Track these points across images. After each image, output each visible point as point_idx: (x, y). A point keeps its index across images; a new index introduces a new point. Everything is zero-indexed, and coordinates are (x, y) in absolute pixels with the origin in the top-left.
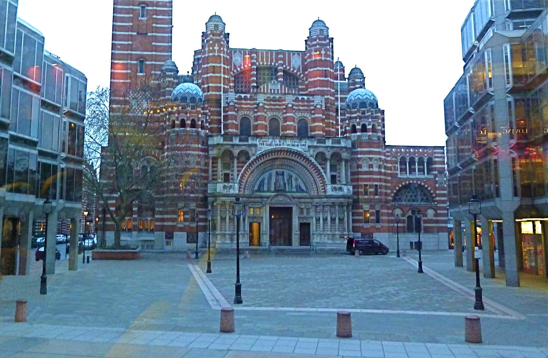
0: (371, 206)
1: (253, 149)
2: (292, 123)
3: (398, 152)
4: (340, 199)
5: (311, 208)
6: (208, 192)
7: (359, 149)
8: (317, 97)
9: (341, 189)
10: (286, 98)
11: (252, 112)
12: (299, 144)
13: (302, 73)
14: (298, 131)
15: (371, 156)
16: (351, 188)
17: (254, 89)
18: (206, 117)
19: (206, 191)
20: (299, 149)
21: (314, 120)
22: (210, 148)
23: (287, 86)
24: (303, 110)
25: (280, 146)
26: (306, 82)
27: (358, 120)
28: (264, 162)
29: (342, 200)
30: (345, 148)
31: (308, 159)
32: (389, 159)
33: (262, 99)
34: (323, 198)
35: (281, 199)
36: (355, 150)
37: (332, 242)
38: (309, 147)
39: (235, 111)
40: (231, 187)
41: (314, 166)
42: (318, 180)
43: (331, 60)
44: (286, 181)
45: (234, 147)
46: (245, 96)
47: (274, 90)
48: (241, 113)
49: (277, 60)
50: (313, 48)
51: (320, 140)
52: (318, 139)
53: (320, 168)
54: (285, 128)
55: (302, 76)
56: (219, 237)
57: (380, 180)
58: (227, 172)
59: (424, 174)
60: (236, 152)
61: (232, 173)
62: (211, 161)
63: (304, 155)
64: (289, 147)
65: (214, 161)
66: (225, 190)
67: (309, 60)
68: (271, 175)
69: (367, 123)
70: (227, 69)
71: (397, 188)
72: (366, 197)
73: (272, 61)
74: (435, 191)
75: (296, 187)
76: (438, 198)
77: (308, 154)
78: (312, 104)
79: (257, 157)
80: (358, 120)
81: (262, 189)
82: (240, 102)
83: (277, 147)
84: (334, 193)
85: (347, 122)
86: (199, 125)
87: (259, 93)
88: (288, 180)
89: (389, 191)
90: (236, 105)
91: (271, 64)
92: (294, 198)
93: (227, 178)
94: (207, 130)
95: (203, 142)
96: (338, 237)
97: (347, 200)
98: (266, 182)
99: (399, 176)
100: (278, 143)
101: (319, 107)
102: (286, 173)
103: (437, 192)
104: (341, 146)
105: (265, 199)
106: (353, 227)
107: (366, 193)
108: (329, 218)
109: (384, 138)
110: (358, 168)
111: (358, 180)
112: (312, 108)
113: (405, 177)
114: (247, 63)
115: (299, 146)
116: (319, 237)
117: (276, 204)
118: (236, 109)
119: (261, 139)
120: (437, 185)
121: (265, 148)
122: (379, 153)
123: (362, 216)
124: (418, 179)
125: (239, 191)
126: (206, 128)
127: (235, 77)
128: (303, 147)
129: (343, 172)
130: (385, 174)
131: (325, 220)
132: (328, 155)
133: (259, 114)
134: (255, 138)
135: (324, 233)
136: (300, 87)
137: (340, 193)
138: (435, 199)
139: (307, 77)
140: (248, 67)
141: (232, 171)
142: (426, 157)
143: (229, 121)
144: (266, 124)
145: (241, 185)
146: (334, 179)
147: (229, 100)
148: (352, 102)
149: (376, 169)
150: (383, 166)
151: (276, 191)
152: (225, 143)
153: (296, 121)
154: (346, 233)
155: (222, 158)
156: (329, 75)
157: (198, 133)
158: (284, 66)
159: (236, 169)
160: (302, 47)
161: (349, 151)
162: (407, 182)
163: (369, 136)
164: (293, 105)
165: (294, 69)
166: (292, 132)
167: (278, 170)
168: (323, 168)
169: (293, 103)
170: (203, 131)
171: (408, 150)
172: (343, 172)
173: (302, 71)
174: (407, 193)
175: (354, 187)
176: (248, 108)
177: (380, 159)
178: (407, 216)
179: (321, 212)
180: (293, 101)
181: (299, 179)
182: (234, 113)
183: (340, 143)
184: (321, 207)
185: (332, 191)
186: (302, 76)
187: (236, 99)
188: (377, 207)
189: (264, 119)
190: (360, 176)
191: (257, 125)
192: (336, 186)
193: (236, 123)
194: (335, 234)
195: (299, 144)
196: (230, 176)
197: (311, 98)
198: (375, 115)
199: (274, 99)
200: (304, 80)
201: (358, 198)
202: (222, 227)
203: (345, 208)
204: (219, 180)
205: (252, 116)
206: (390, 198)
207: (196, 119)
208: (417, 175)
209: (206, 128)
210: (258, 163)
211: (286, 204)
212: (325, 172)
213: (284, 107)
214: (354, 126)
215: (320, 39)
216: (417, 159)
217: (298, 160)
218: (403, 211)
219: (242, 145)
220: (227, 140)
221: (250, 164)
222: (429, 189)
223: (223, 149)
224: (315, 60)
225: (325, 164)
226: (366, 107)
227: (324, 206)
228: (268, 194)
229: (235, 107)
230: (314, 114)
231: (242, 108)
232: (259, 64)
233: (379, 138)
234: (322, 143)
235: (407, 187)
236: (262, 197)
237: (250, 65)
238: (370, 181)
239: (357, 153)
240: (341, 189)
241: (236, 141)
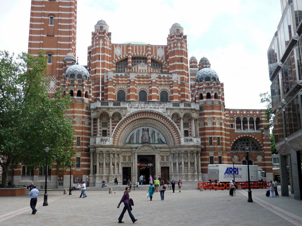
0: (214, 153)
1: (124, 111)
2: (155, 94)
3: (235, 114)
4: (191, 148)
5: (170, 155)
6: (90, 144)
7: (205, 111)
8: (174, 75)
9: (191, 140)
10: (152, 76)
11: (126, 86)
12: (159, 107)
13: (165, 61)
14: (161, 100)
15: (214, 116)
16: (199, 140)
17: (128, 69)
18: (90, 89)
19: (89, 144)
20: (160, 111)
21: (172, 92)
22: (92, 111)
23: (153, 67)
24: (164, 84)
25: (145, 109)
26: (168, 67)
27: (204, 90)
28: (133, 121)
29: (193, 148)
30: (194, 109)
31: (166, 118)
32: (228, 119)
33: (133, 77)
34: (179, 147)
35: (146, 149)
36: (203, 112)
37: (185, 181)
38: (167, 109)
39: (113, 86)
40: (106, 140)
41: (171, 123)
42: (174, 134)
43: (185, 50)
44: (150, 136)
45: (109, 110)
46: (121, 75)
47: (143, 70)
48: (117, 88)
49: (147, 51)
50: (172, 42)
51: (175, 104)
52: (173, 104)
53: (175, 125)
54: (151, 97)
55: (165, 62)
56: (97, 178)
57: (221, 134)
58: (105, 129)
59: (254, 130)
60: (111, 114)
61: (108, 130)
62: (92, 121)
63: (163, 116)
64: (151, 109)
65: (95, 122)
66: (102, 142)
67: (169, 51)
68: (139, 131)
69: (210, 92)
70: (110, 57)
71: (235, 140)
72: (211, 146)
73: (143, 52)
74: (262, 143)
75: (158, 140)
76: (264, 147)
77: (166, 115)
78: (171, 80)
79: (127, 117)
80: (204, 90)
81: (132, 142)
82: (117, 79)
83: (143, 109)
84: (186, 144)
85: (196, 91)
86: (83, 94)
87: (131, 72)
88: (152, 135)
89: (229, 143)
90: (114, 81)
91: (142, 55)
92: (156, 148)
93: (105, 133)
94: (90, 98)
95: (87, 107)
96: (190, 177)
97: (196, 148)
98: (135, 136)
99: (236, 131)
100: (143, 106)
101: (175, 81)
102: (150, 129)
103: (264, 143)
104: (191, 108)
105: (135, 149)
106: (202, 169)
107: (211, 144)
108: (183, 163)
109: (224, 104)
110: (204, 125)
111: (204, 134)
112: (171, 83)
113: (240, 132)
114: (125, 54)
115: (160, 109)
116: (175, 177)
117: (141, 153)
118: (114, 84)
119: (130, 103)
120: (264, 138)
121: (133, 110)
122: (220, 114)
123: (209, 161)
124: (250, 134)
125: (114, 143)
126: (90, 97)
127: (116, 64)
128: (163, 109)
129: (194, 128)
130: (225, 130)
131: (180, 164)
132: (182, 115)
133: (131, 87)
134: (125, 103)
135: (179, 174)
136: (164, 70)
137: (191, 144)
138: (262, 148)
139: (168, 63)
140: (126, 56)
141: (109, 128)
142: (255, 117)
143: (109, 93)
144: (136, 94)
145: (115, 138)
146: (186, 133)
147: (108, 78)
148: (200, 77)
149: (218, 126)
150: (223, 124)
151: (143, 143)
152: (102, 107)
153: (159, 92)
154: (196, 173)
155: (101, 119)
156: (184, 60)
157: (83, 100)
158: (152, 56)
159: (111, 127)
160: (165, 43)
161: (198, 113)
162: (242, 136)
163: (212, 101)
164: (157, 81)
165: (159, 58)
166: (156, 100)
167: (144, 127)
168: (178, 125)
169: (157, 79)
170: (88, 99)
171: (242, 112)
172: (194, 128)
174: (242, 144)
175: (202, 139)
176: (123, 83)
177: (221, 118)
178: (242, 160)
179: (177, 158)
180: (157, 78)
181: (160, 134)
182: (112, 87)
183: (190, 106)
184: (177, 155)
185: (185, 142)
186: (165, 62)
187: (114, 77)
188: (220, 154)
189: (135, 91)
190: (206, 131)
191: (129, 95)
192: (187, 138)
193: (114, 94)
194: (188, 175)
195: (159, 107)
196: (108, 133)
197: (170, 75)
198: (216, 86)
199: (142, 77)
200: (166, 66)
201: (205, 148)
202: (100, 170)
203: (195, 154)
204: (98, 135)
205: (126, 89)
206: (230, 148)
207: (81, 90)
208: (249, 131)
209: (90, 97)
210: (128, 122)
211: (149, 153)
212: (179, 128)
213: (150, 82)
214: (201, 95)
215: (177, 36)
216: (248, 119)
217: (159, 119)
218: (239, 158)
219: (115, 108)
220: (104, 105)
221: (121, 122)
222: (258, 140)
223: (100, 111)
224: (174, 51)
225: (179, 122)
226: (209, 80)
227: (179, 154)
228: (136, 145)
229: (114, 83)
230: (172, 87)
231: (118, 83)
232: (134, 55)
233: (220, 103)
234: (177, 106)
235: (241, 139)
236: (132, 148)
237: (127, 55)
238: (214, 135)
239: (204, 114)
240: (191, 140)
241: (111, 105)
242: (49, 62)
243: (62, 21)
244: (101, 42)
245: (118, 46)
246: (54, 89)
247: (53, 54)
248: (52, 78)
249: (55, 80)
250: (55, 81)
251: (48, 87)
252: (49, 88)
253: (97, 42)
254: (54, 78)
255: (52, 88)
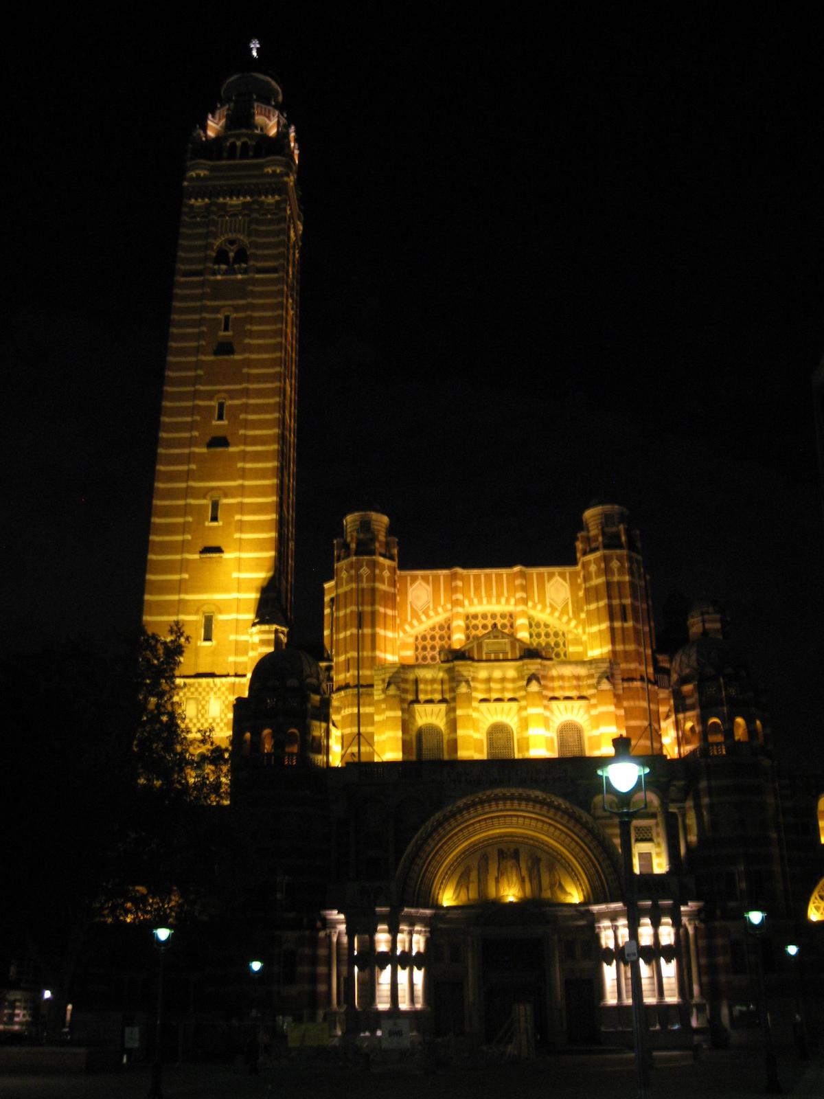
114: (442, 602)
173: (573, 612)
242: (208, 638)
243: (242, 508)
244: (365, 571)
245: (420, 577)
246: (222, 725)
247: (220, 612)
248: (215, 689)
249: (223, 693)
250: (223, 698)
251: (203, 716)
252: (206, 720)
253: (353, 572)
254: (219, 689)
255: (214, 720)
